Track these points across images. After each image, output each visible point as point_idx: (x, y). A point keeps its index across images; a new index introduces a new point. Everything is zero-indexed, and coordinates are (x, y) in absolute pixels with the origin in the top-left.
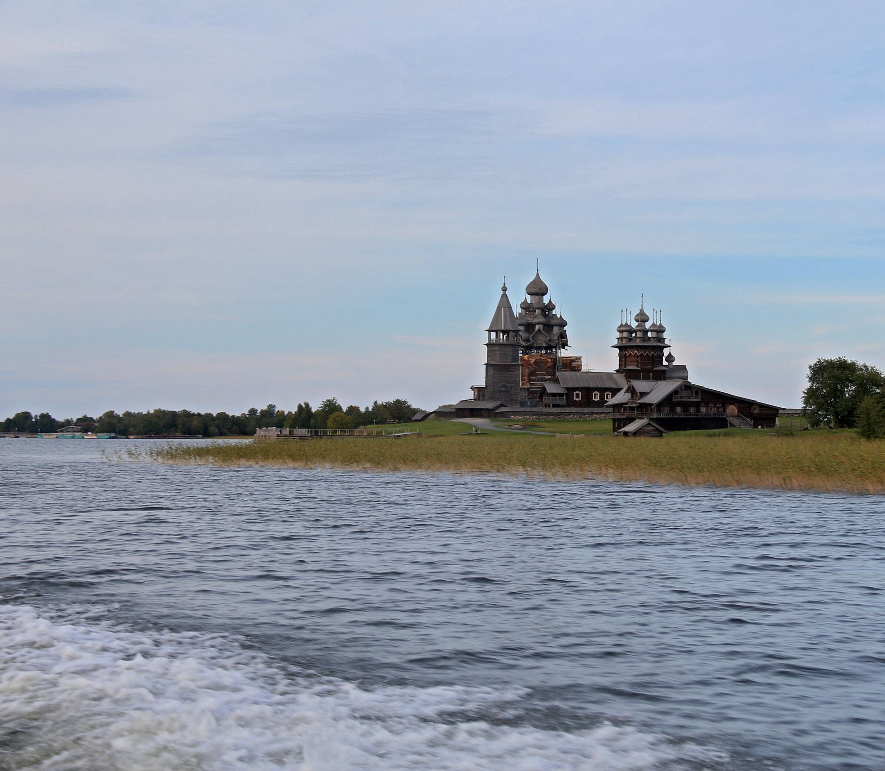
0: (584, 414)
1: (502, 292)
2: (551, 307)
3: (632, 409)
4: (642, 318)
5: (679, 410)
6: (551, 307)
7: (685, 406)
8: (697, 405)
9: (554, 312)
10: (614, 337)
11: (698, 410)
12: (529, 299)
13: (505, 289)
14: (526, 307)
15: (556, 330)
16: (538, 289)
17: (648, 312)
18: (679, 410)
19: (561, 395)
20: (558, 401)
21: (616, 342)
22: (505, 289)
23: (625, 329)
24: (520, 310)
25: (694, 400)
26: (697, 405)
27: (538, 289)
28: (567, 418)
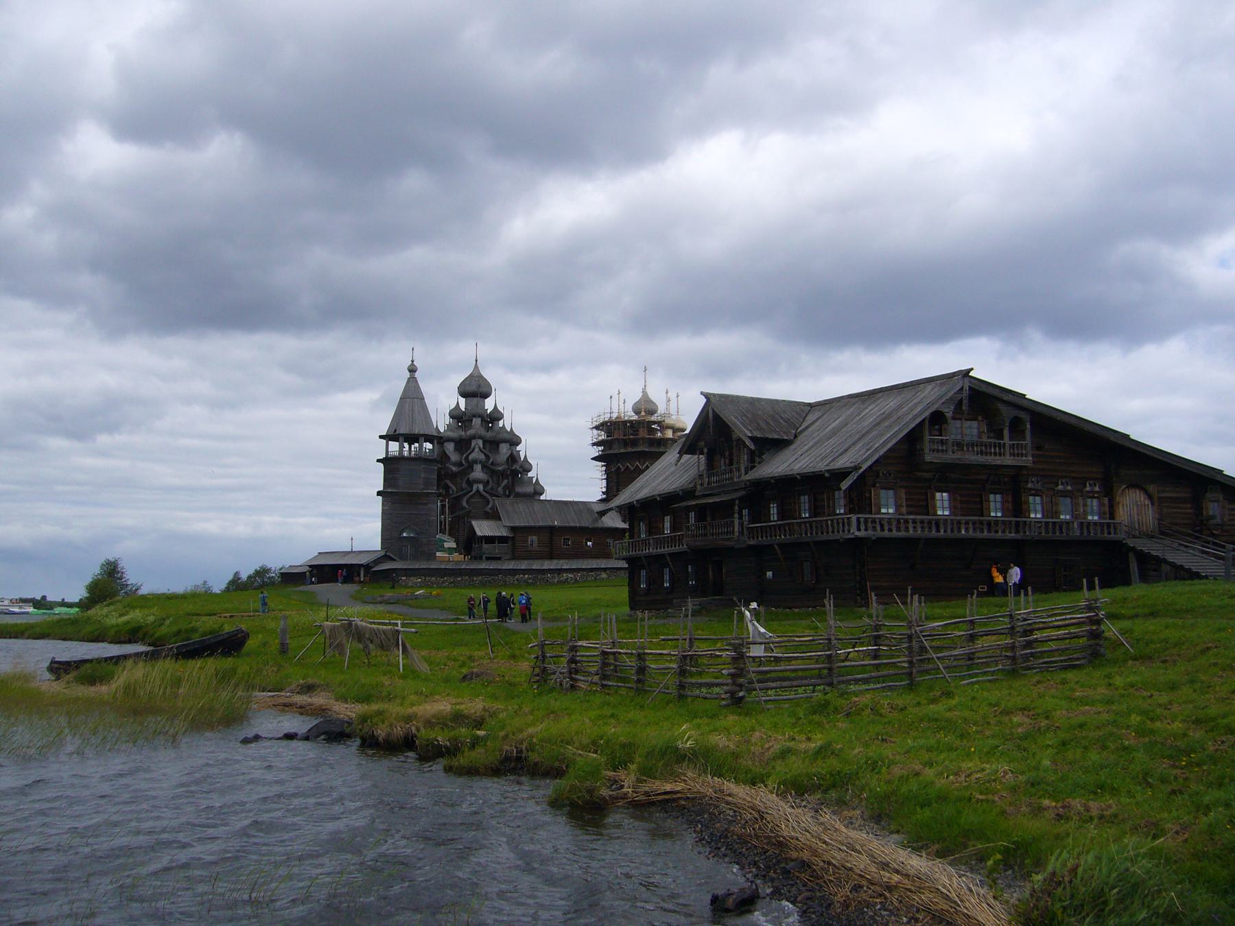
0: (543, 571)
1: (408, 375)
2: (496, 415)
3: (724, 510)
5: (942, 504)
6: (496, 416)
7: (969, 484)
8: (1014, 485)
9: (501, 424)
11: (1018, 508)
12: (462, 402)
13: (412, 370)
14: (456, 415)
15: (504, 448)
16: (475, 389)
18: (942, 504)
19: (502, 540)
20: (497, 549)
24: (448, 420)
25: (1008, 460)
26: (1014, 485)
27: (475, 389)
28: (509, 579)
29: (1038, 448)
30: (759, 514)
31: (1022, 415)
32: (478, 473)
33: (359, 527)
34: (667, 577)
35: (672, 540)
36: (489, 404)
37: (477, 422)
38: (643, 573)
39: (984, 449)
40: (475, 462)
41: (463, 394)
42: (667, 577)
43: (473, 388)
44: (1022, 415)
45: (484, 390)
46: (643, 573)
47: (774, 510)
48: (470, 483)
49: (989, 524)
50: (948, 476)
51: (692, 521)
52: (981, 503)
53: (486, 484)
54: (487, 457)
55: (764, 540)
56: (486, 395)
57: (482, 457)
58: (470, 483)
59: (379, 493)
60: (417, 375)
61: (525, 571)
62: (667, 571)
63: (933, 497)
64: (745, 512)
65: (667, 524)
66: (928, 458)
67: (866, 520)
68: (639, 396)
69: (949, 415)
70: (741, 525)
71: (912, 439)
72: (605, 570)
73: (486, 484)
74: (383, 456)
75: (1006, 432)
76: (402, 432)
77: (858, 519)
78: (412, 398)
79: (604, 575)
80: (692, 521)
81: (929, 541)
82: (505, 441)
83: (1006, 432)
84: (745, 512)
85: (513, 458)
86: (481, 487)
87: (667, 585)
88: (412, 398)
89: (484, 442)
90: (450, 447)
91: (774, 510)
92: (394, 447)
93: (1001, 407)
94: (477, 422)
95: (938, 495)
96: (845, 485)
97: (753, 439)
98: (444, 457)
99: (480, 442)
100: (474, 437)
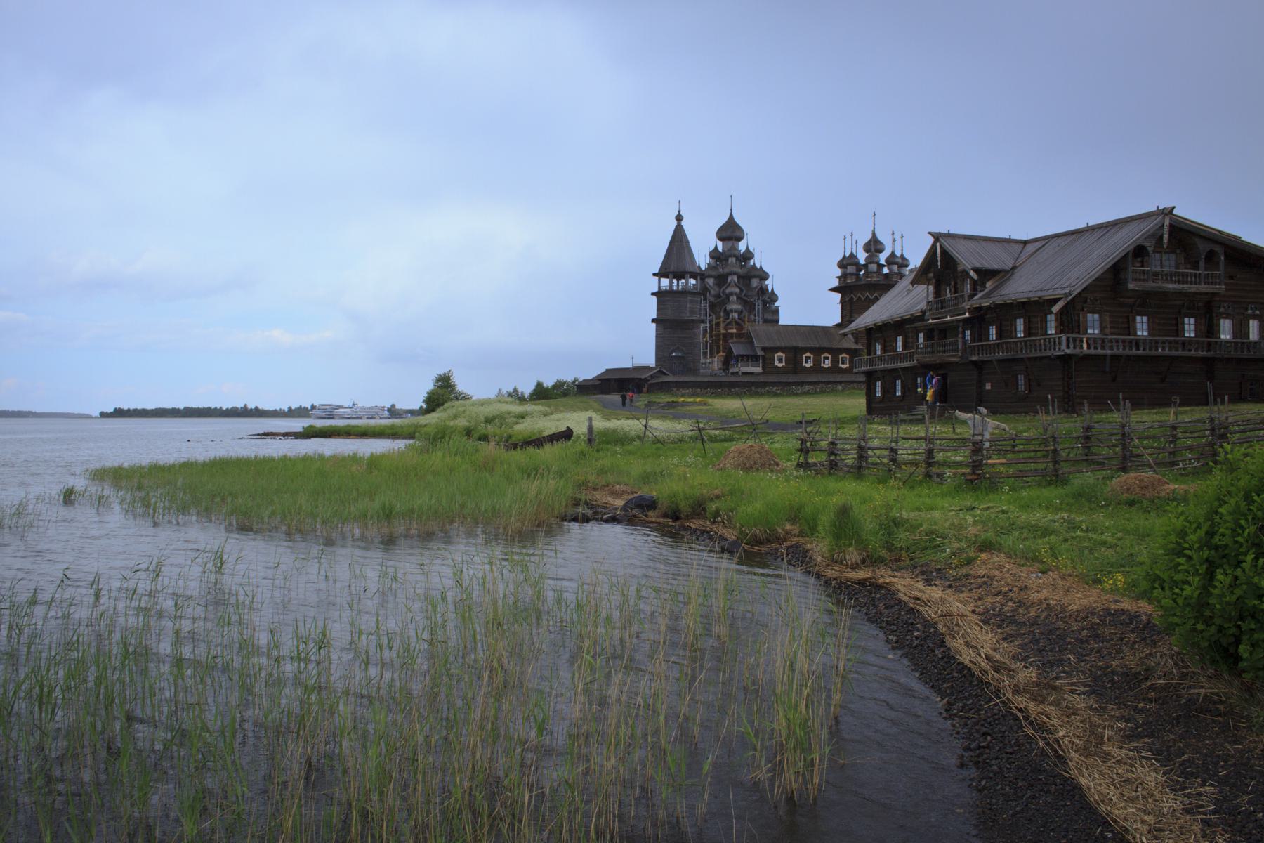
0: (789, 384)
1: (675, 223)
4: (874, 246)
5: (1142, 327)
6: (748, 255)
7: (1166, 310)
9: (752, 262)
10: (832, 275)
11: (1210, 330)
13: (679, 218)
14: (714, 254)
15: (755, 283)
16: (730, 232)
17: (884, 238)
18: (1142, 327)
21: (836, 283)
22: (679, 218)
23: (847, 263)
24: (708, 260)
25: (1203, 288)
26: (1207, 312)
27: (730, 232)
29: (1231, 278)
30: (981, 335)
31: (1217, 249)
32: (734, 305)
33: (638, 347)
34: (899, 387)
35: (902, 357)
36: (742, 247)
37: (732, 260)
38: (879, 384)
39: (1181, 279)
40: (731, 294)
41: (720, 239)
42: (899, 387)
43: (728, 234)
44: (1217, 249)
45: (738, 234)
46: (879, 384)
47: (993, 331)
48: (727, 313)
49: (1183, 343)
50: (1147, 302)
51: (921, 340)
52: (1177, 325)
53: (740, 312)
54: (741, 290)
55: (985, 357)
56: (740, 239)
57: (737, 290)
58: (727, 313)
59: (653, 321)
60: (683, 223)
61: (773, 384)
62: (899, 382)
63: (1134, 320)
64: (968, 333)
65: (900, 344)
66: (1131, 286)
67: (1074, 340)
68: (868, 237)
69: (1150, 249)
70: (964, 342)
71: (1117, 270)
72: (840, 383)
73: (740, 312)
74: (656, 290)
75: (1202, 264)
76: (672, 269)
77: (1068, 339)
78: (679, 241)
79: (840, 388)
80: (921, 340)
81: (1129, 357)
82: (755, 277)
83: (1202, 264)
84: (968, 333)
85: (763, 290)
86: (736, 315)
87: (899, 393)
88: (679, 241)
89: (739, 277)
90: (710, 282)
91: (993, 331)
92: (665, 282)
93: (1198, 241)
94: (732, 260)
95: (1138, 318)
96: (1056, 309)
97: (977, 271)
98: (705, 290)
99: (735, 278)
100: (730, 274)
